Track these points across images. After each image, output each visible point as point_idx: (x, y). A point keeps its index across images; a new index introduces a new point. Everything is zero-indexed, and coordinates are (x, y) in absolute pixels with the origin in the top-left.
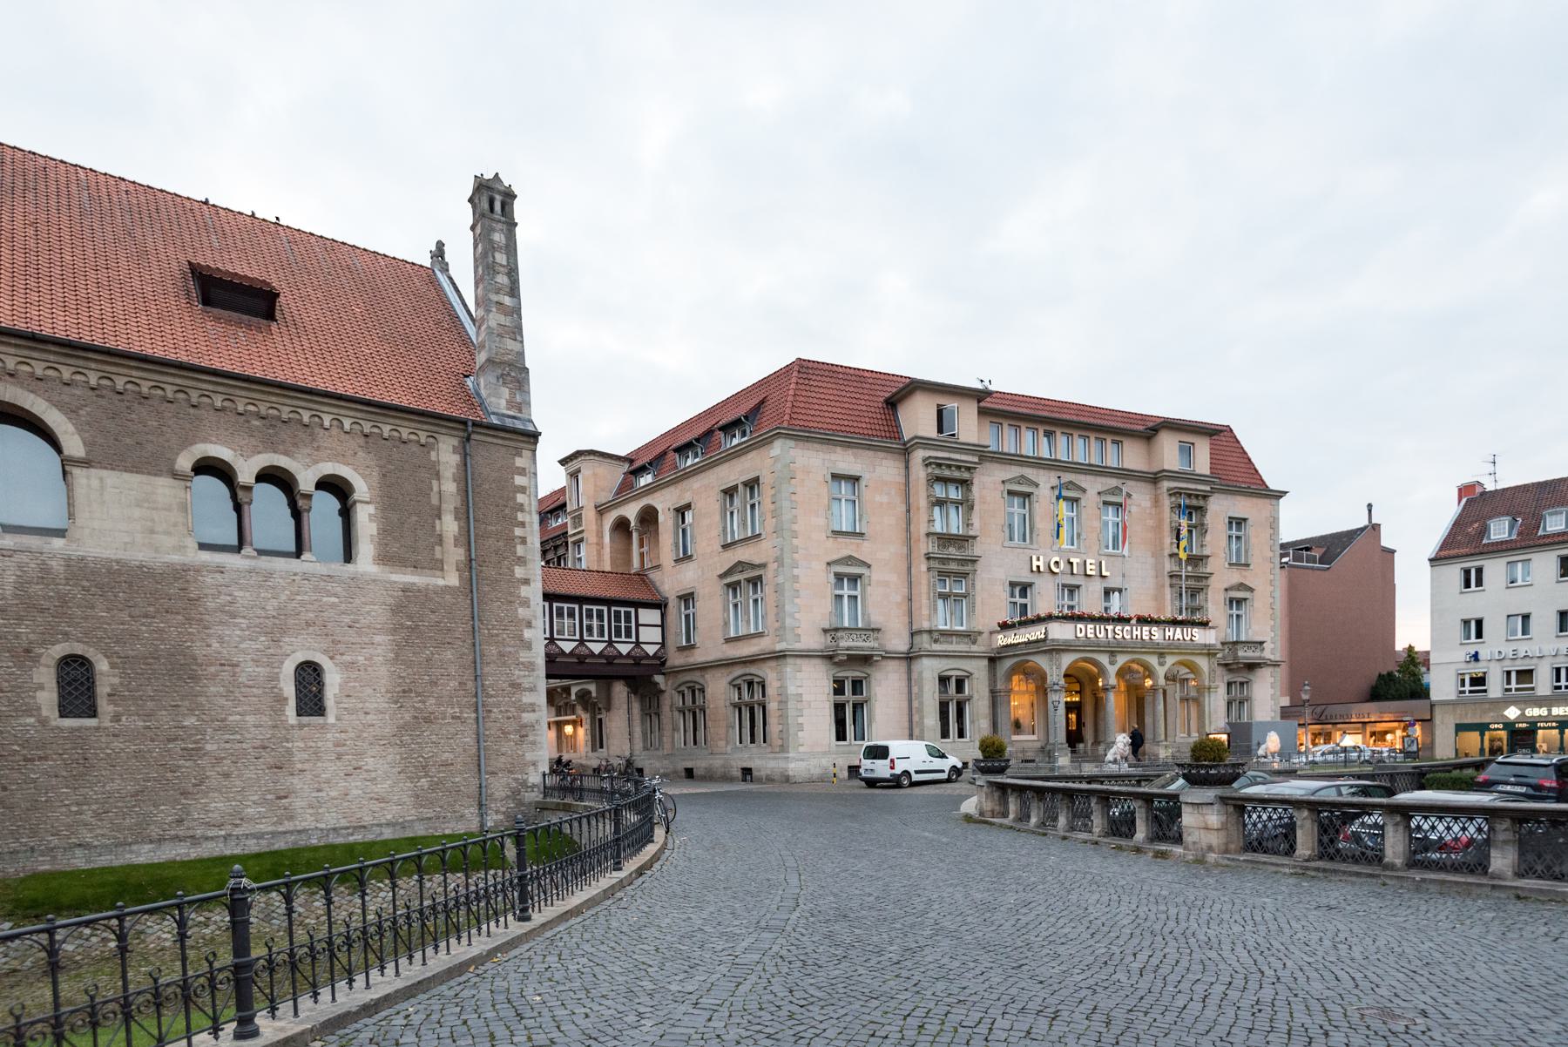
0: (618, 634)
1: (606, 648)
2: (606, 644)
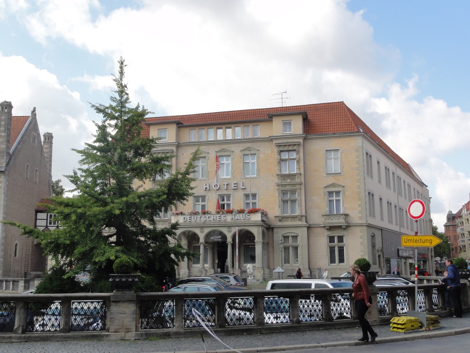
0: (50, 223)
1: (45, 229)
2: (56, 227)
